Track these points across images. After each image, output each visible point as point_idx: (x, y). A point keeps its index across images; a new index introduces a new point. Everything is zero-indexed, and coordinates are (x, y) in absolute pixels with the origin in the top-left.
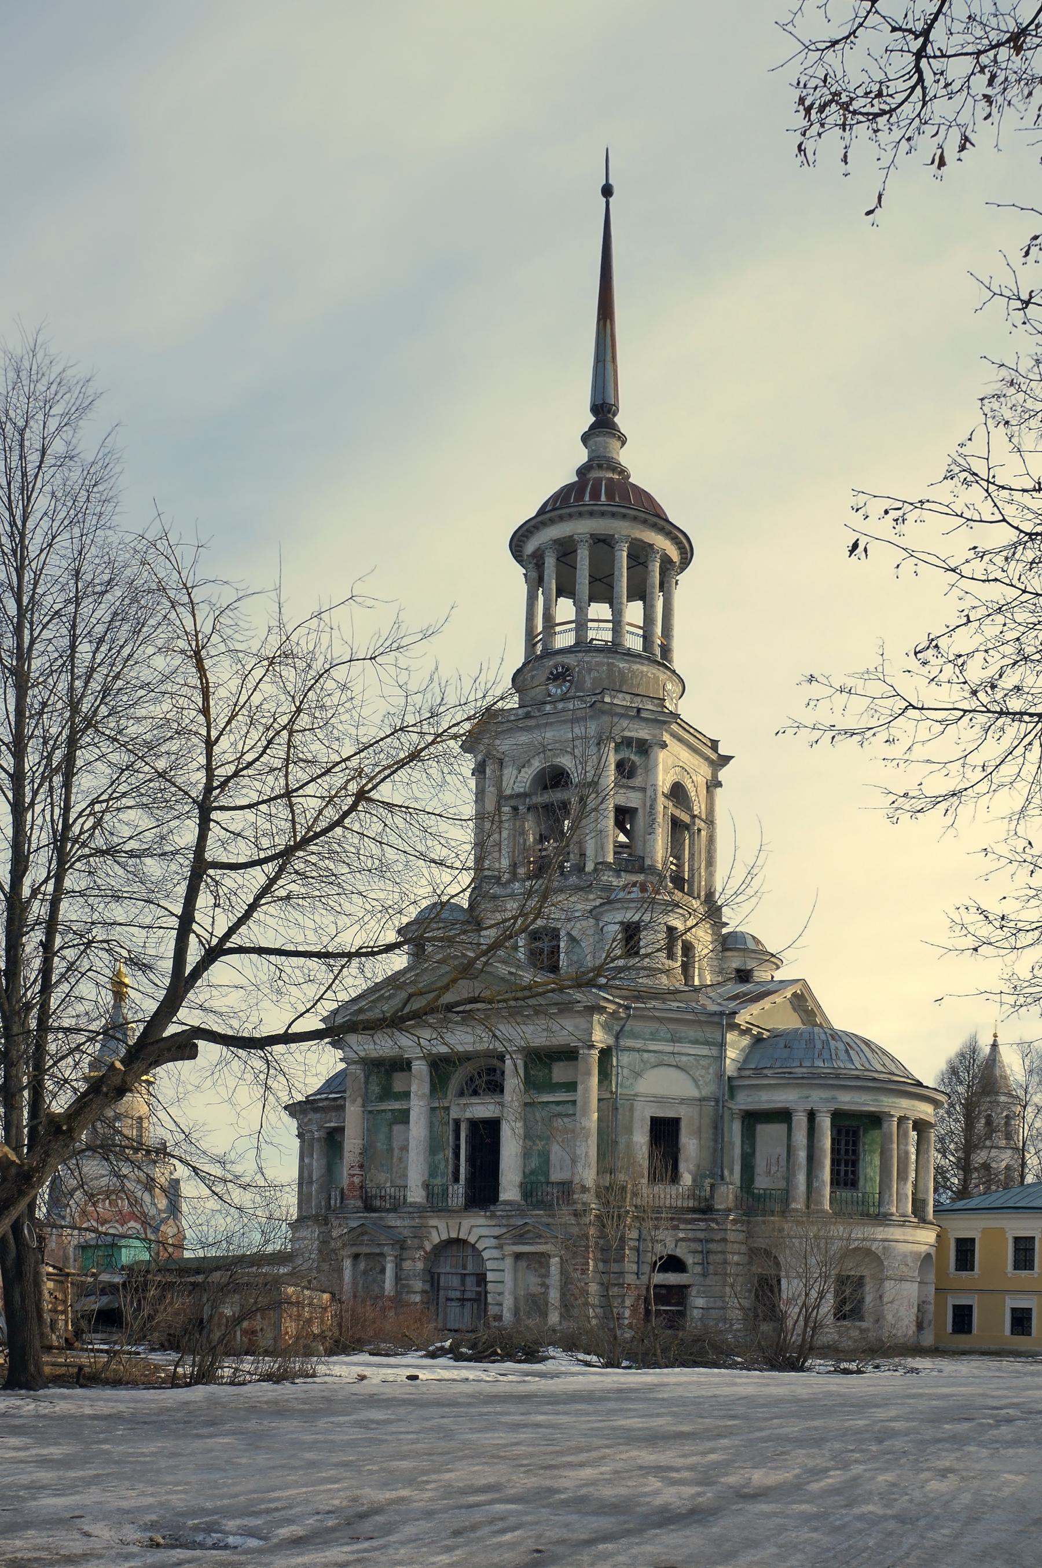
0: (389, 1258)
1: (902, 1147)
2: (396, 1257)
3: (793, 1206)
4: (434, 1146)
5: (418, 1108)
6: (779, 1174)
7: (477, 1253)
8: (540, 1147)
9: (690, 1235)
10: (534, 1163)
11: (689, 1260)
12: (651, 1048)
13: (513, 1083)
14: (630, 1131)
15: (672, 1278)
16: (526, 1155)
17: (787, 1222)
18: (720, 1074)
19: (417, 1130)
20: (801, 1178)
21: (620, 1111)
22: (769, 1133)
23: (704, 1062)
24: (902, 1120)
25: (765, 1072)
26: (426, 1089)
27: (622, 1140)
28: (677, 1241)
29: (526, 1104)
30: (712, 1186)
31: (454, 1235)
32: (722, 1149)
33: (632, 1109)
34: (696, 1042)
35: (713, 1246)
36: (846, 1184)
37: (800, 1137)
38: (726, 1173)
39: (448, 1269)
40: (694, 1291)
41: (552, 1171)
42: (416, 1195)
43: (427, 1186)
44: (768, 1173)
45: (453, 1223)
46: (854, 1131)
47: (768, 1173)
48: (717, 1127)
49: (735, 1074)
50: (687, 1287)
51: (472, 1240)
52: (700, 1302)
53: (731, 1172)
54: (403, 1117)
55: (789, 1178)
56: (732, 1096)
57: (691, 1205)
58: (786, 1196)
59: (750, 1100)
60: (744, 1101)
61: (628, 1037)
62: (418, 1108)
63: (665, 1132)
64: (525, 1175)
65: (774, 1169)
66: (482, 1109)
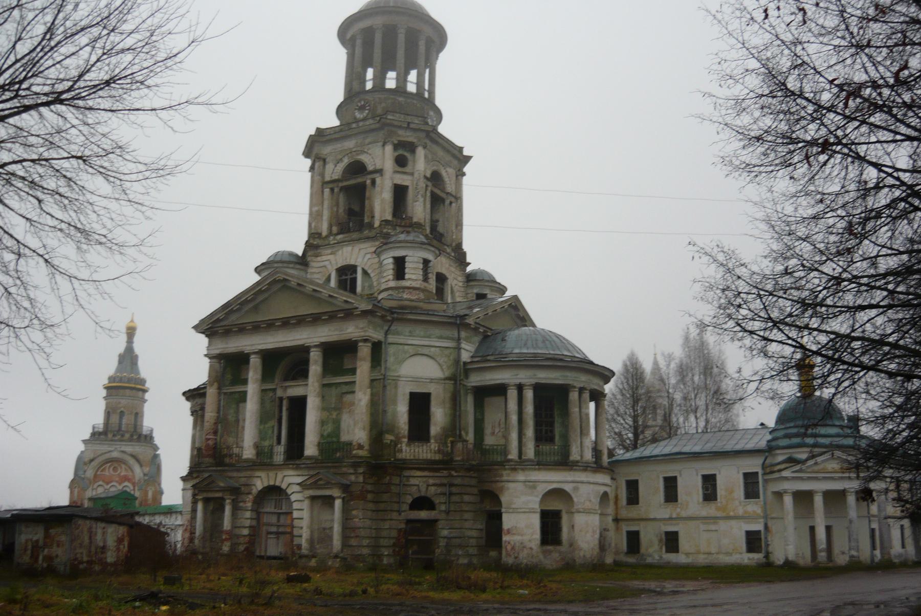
0: (228, 501)
1: (583, 410)
2: (233, 500)
3: (510, 457)
4: (263, 418)
5: (252, 389)
6: (500, 434)
7: (287, 497)
8: (334, 417)
9: (437, 481)
10: (329, 428)
11: (436, 501)
12: (410, 342)
13: (315, 368)
14: (395, 402)
15: (423, 514)
16: (323, 423)
17: (505, 469)
18: (457, 361)
19: (251, 406)
20: (514, 436)
21: (388, 388)
22: (493, 403)
23: (447, 352)
24: (581, 390)
25: (489, 358)
26: (259, 376)
27: (390, 409)
28: (428, 486)
29: (324, 385)
30: (452, 442)
31: (272, 483)
32: (460, 416)
33: (396, 387)
34: (441, 337)
35: (454, 490)
36: (546, 440)
37: (512, 405)
38: (463, 433)
39: (268, 510)
40: (441, 524)
41: (342, 434)
42: (248, 452)
43: (256, 446)
44: (493, 434)
45: (272, 474)
46: (552, 404)
47: (493, 434)
48: (455, 401)
49: (469, 360)
50: (436, 521)
51: (284, 486)
52: (445, 533)
53: (467, 433)
54: (243, 397)
55: (506, 437)
56: (467, 376)
57: (437, 458)
58: (505, 451)
59: (479, 379)
60: (476, 380)
61: (394, 334)
62: (252, 389)
63: (420, 404)
64: (322, 436)
65: (497, 430)
66: (296, 391)
